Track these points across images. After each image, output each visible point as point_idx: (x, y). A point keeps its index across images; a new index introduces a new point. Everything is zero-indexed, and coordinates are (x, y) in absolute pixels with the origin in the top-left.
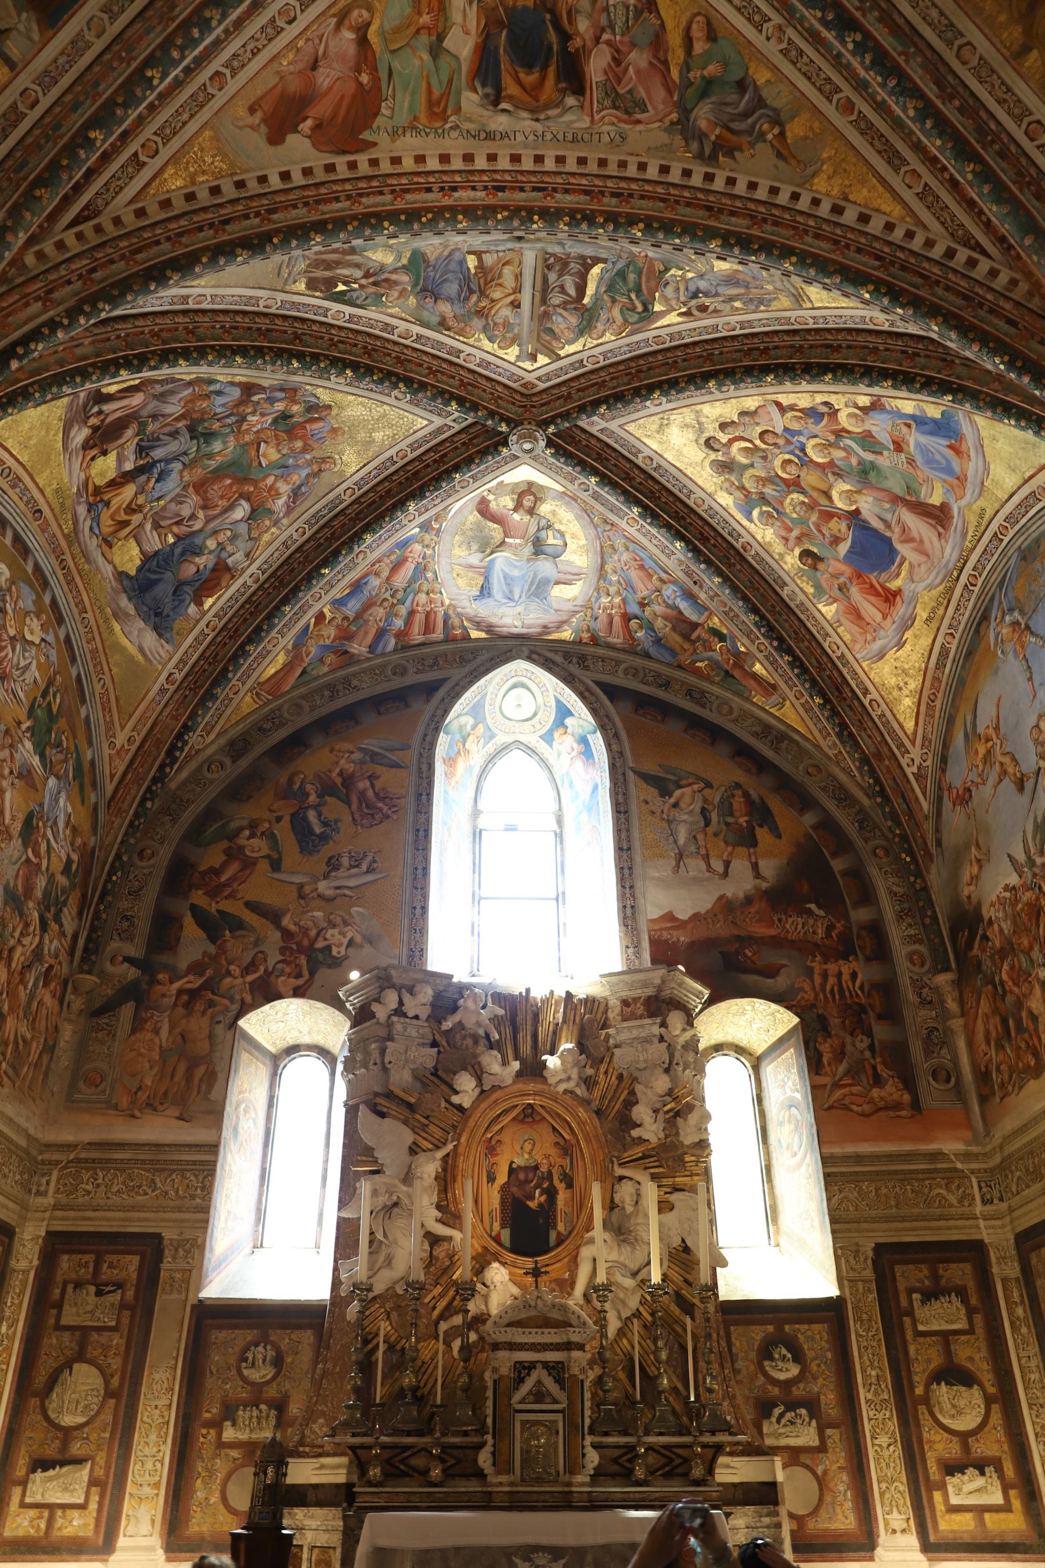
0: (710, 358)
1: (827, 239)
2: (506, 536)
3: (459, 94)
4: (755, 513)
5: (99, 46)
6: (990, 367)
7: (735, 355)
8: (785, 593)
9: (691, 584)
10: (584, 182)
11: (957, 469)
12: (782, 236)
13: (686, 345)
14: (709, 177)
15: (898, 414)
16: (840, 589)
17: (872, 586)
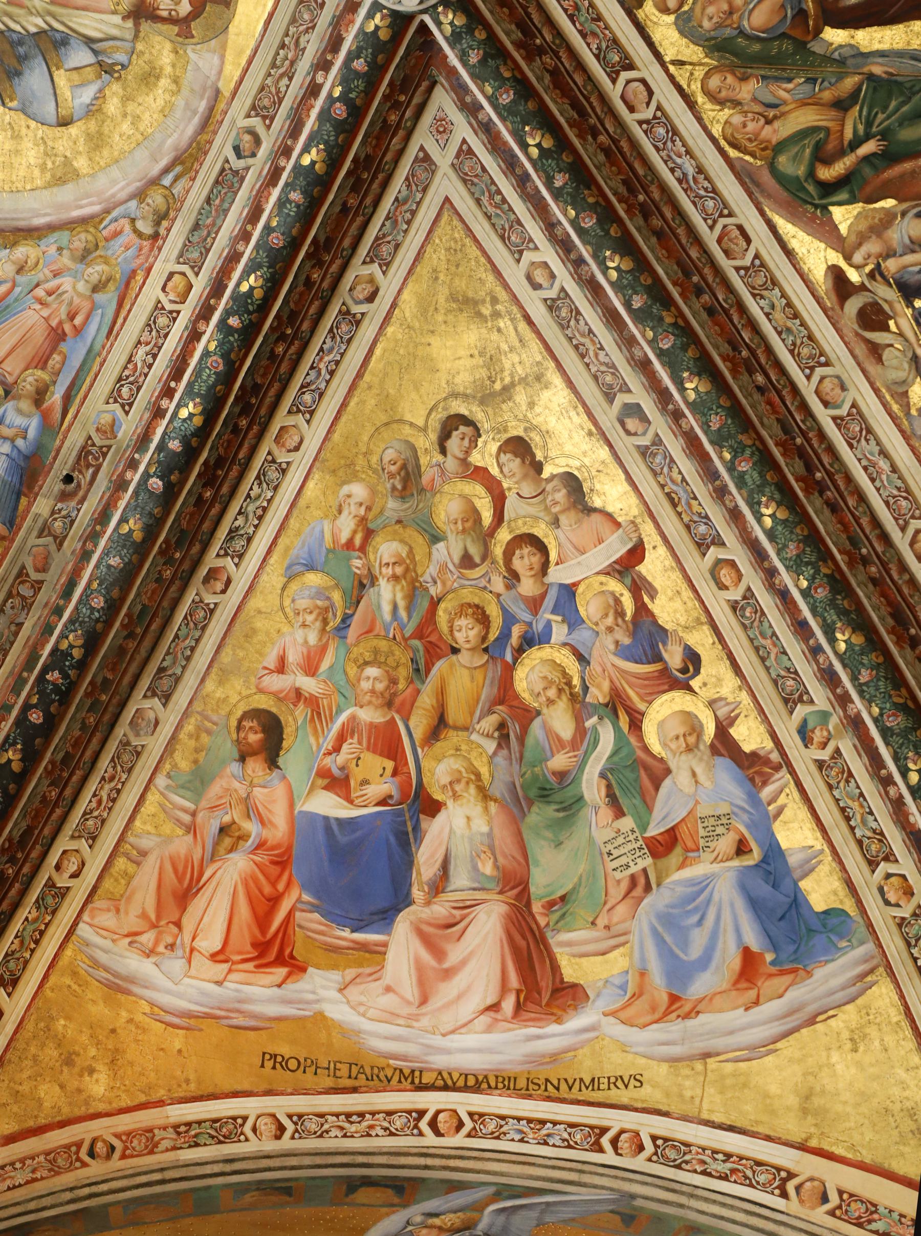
4: (314, 579)
9: (62, 466)
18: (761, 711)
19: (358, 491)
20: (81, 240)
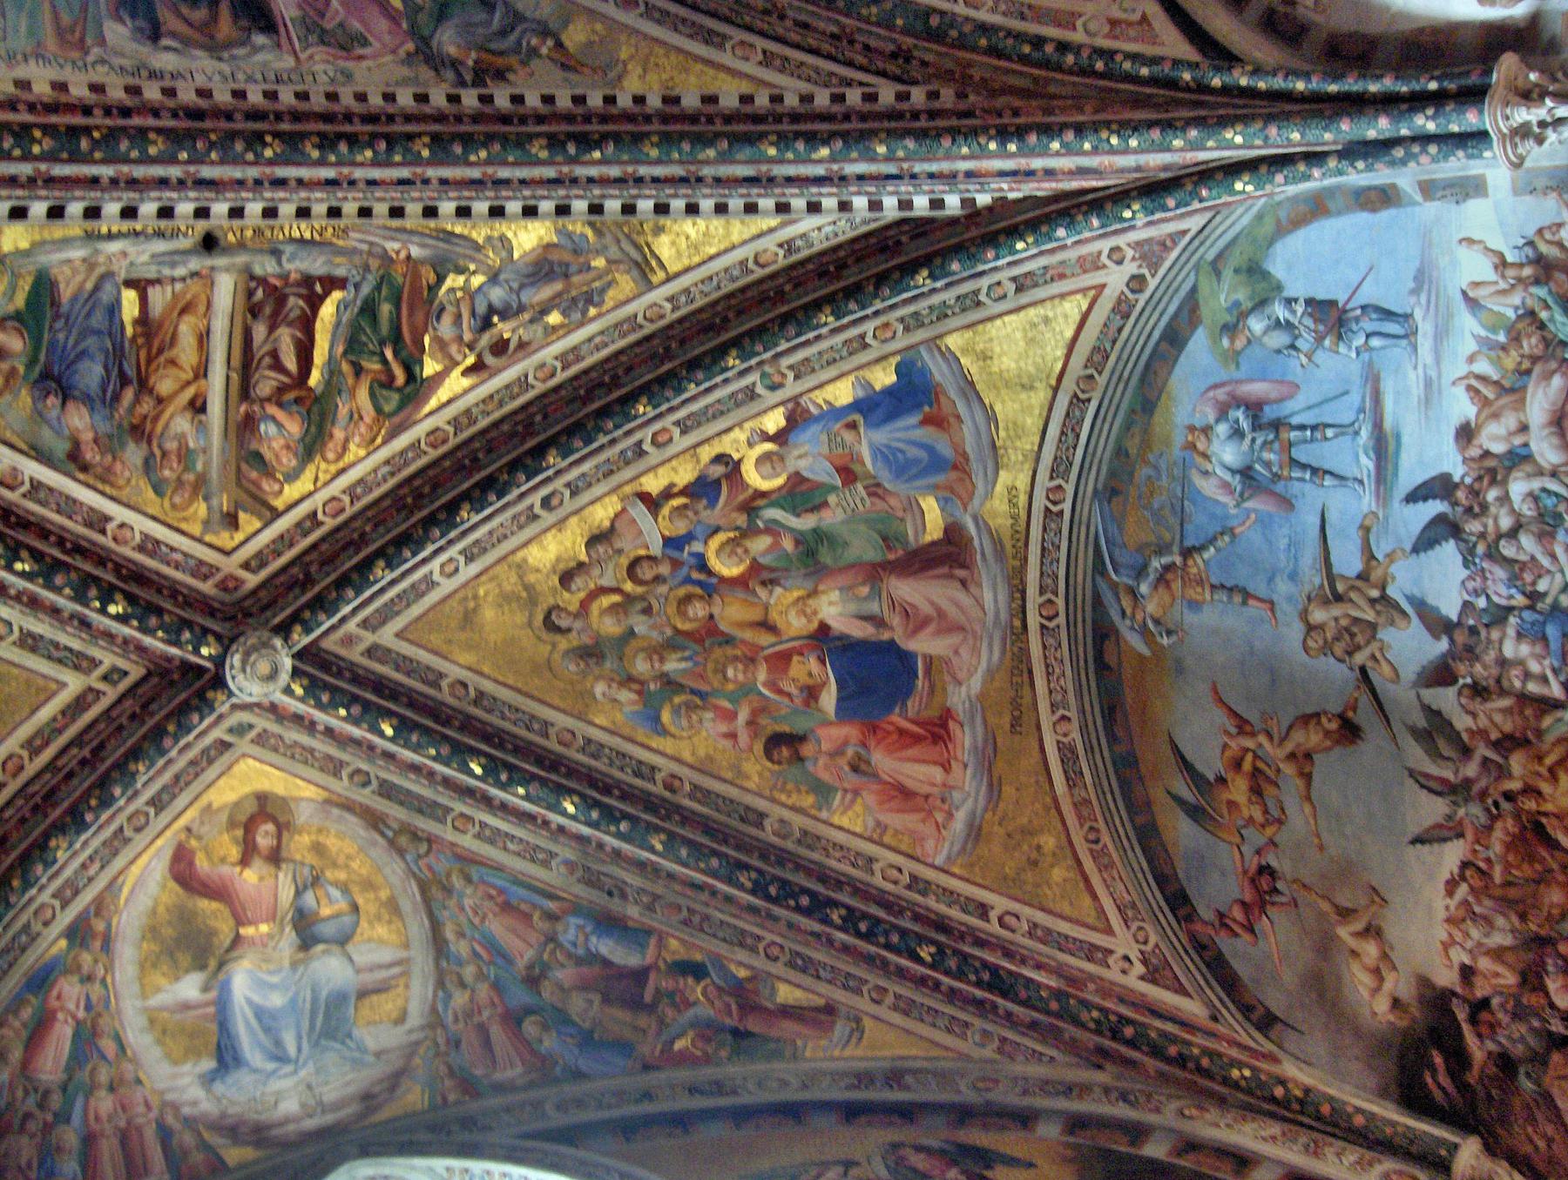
2: (240, 921)
4: (666, 716)
8: (768, 834)
11: (946, 450)
15: (835, 413)
16: (855, 769)
17: (902, 732)
18: (759, 414)
19: (600, 689)
20: (436, 892)
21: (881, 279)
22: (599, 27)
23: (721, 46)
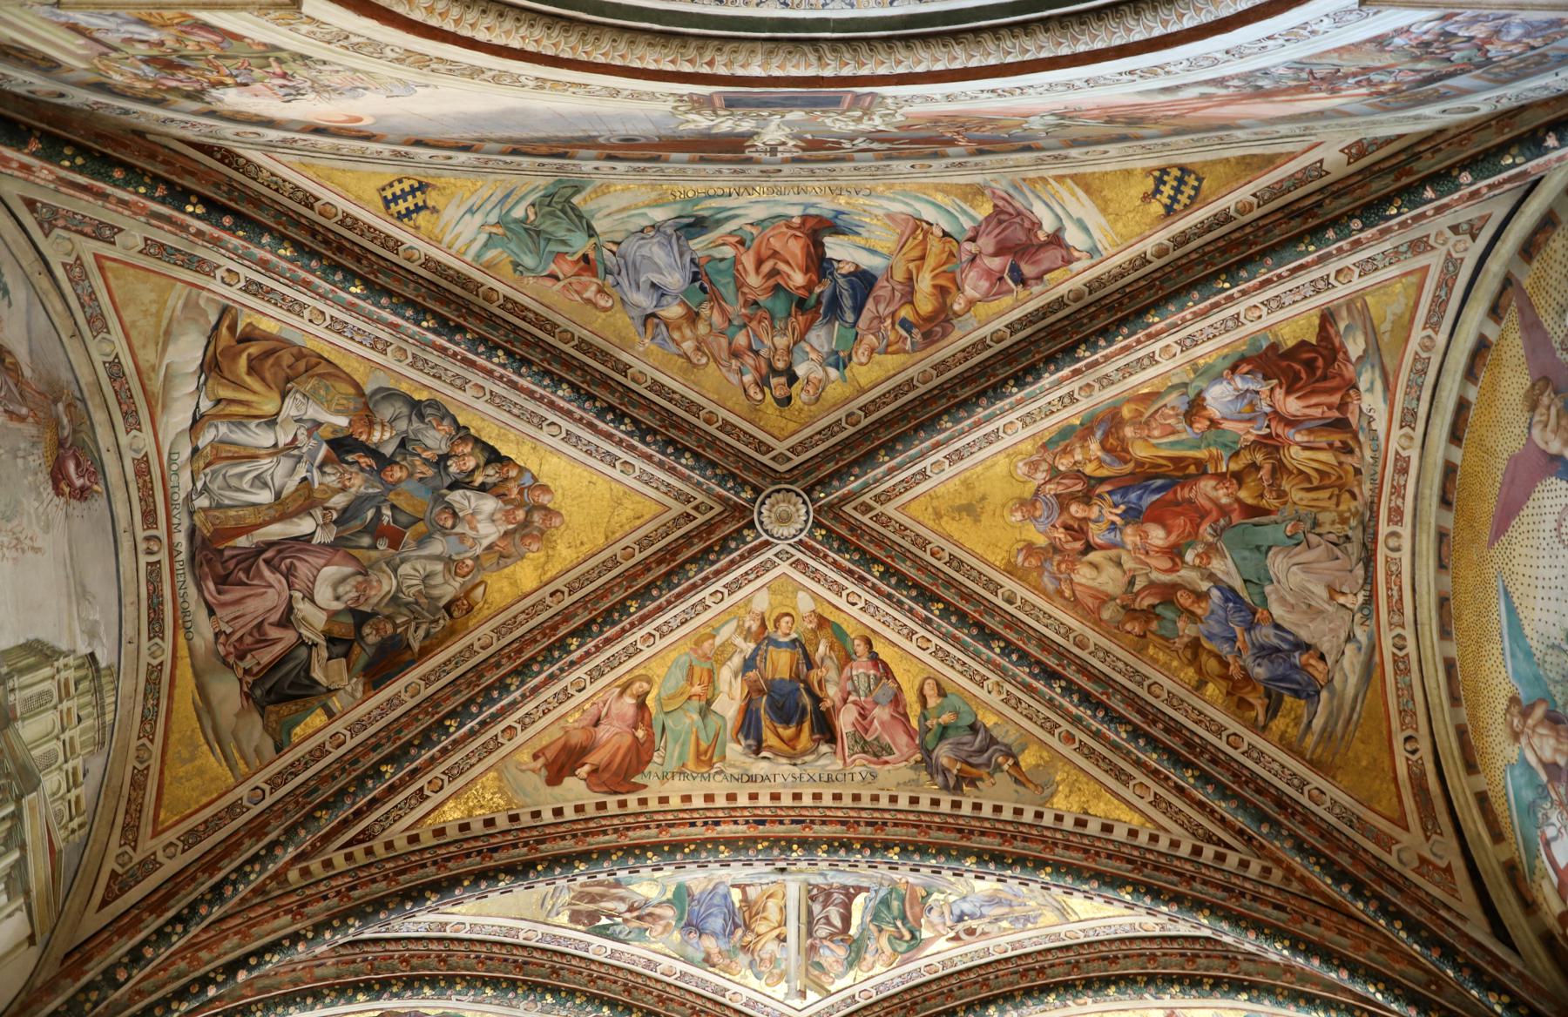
0: (985, 983)
1: (1078, 849)
3: (724, 745)
5: (411, 703)
6: (1275, 958)
7: (1011, 978)
10: (840, 813)
12: (1034, 850)
13: (960, 972)
14: (956, 805)
21: (1217, 983)
22: (1045, 754)
23: (1126, 784)
